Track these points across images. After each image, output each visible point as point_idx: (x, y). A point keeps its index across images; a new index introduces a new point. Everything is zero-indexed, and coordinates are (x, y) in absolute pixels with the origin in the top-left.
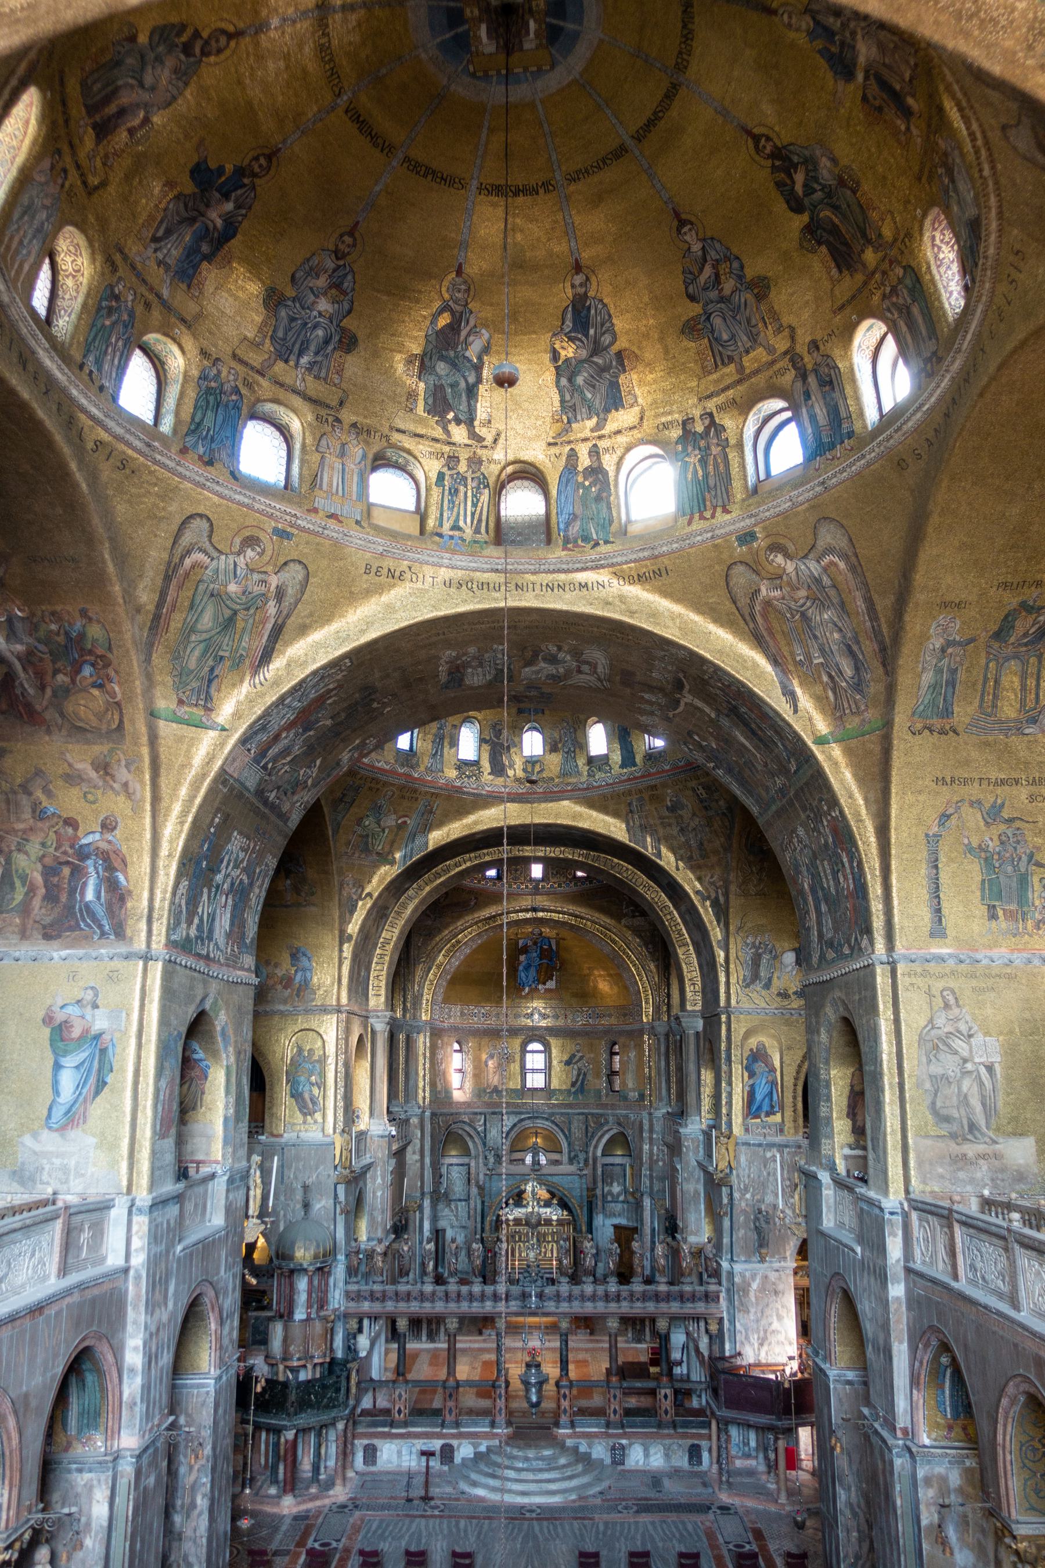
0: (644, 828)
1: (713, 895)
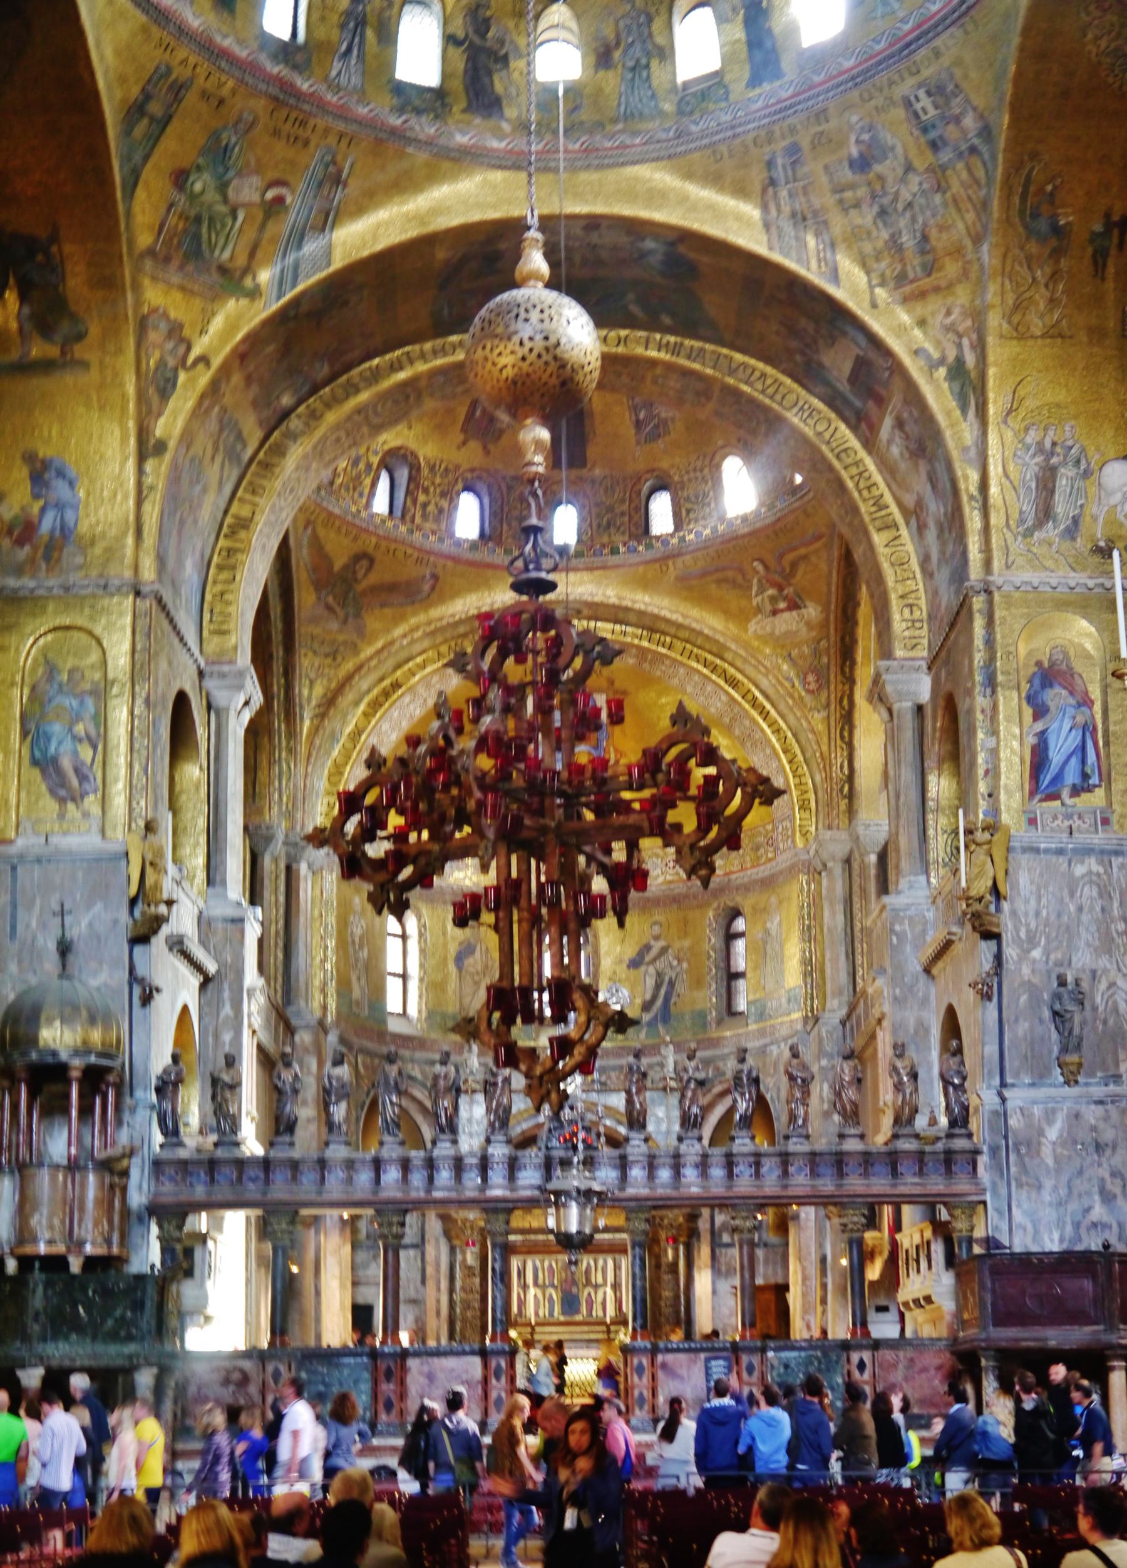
0: (799, 219)
1: (951, 355)
